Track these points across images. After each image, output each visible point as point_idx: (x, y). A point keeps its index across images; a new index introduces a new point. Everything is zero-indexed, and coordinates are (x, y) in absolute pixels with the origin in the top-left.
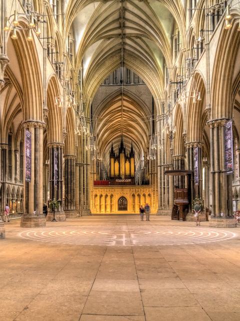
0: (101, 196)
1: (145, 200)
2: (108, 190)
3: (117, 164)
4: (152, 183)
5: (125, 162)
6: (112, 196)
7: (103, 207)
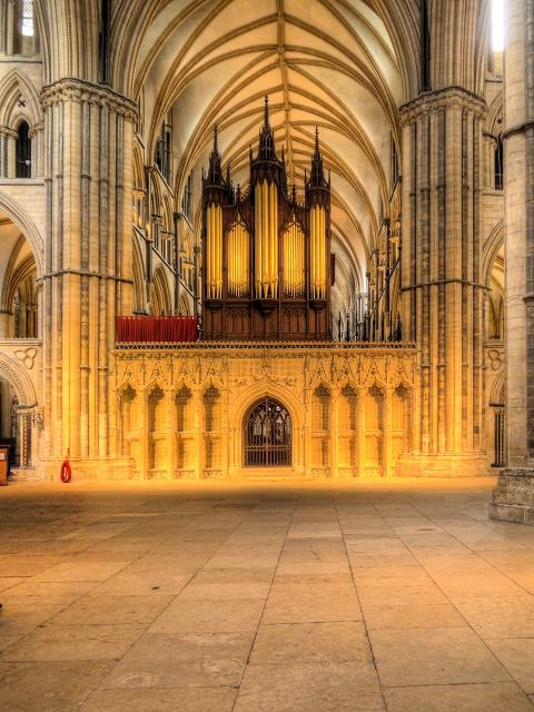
0: (155, 395)
1: (381, 415)
2: (191, 363)
3: (239, 236)
4: (413, 335)
5: (282, 229)
6: (211, 395)
7: (166, 449)
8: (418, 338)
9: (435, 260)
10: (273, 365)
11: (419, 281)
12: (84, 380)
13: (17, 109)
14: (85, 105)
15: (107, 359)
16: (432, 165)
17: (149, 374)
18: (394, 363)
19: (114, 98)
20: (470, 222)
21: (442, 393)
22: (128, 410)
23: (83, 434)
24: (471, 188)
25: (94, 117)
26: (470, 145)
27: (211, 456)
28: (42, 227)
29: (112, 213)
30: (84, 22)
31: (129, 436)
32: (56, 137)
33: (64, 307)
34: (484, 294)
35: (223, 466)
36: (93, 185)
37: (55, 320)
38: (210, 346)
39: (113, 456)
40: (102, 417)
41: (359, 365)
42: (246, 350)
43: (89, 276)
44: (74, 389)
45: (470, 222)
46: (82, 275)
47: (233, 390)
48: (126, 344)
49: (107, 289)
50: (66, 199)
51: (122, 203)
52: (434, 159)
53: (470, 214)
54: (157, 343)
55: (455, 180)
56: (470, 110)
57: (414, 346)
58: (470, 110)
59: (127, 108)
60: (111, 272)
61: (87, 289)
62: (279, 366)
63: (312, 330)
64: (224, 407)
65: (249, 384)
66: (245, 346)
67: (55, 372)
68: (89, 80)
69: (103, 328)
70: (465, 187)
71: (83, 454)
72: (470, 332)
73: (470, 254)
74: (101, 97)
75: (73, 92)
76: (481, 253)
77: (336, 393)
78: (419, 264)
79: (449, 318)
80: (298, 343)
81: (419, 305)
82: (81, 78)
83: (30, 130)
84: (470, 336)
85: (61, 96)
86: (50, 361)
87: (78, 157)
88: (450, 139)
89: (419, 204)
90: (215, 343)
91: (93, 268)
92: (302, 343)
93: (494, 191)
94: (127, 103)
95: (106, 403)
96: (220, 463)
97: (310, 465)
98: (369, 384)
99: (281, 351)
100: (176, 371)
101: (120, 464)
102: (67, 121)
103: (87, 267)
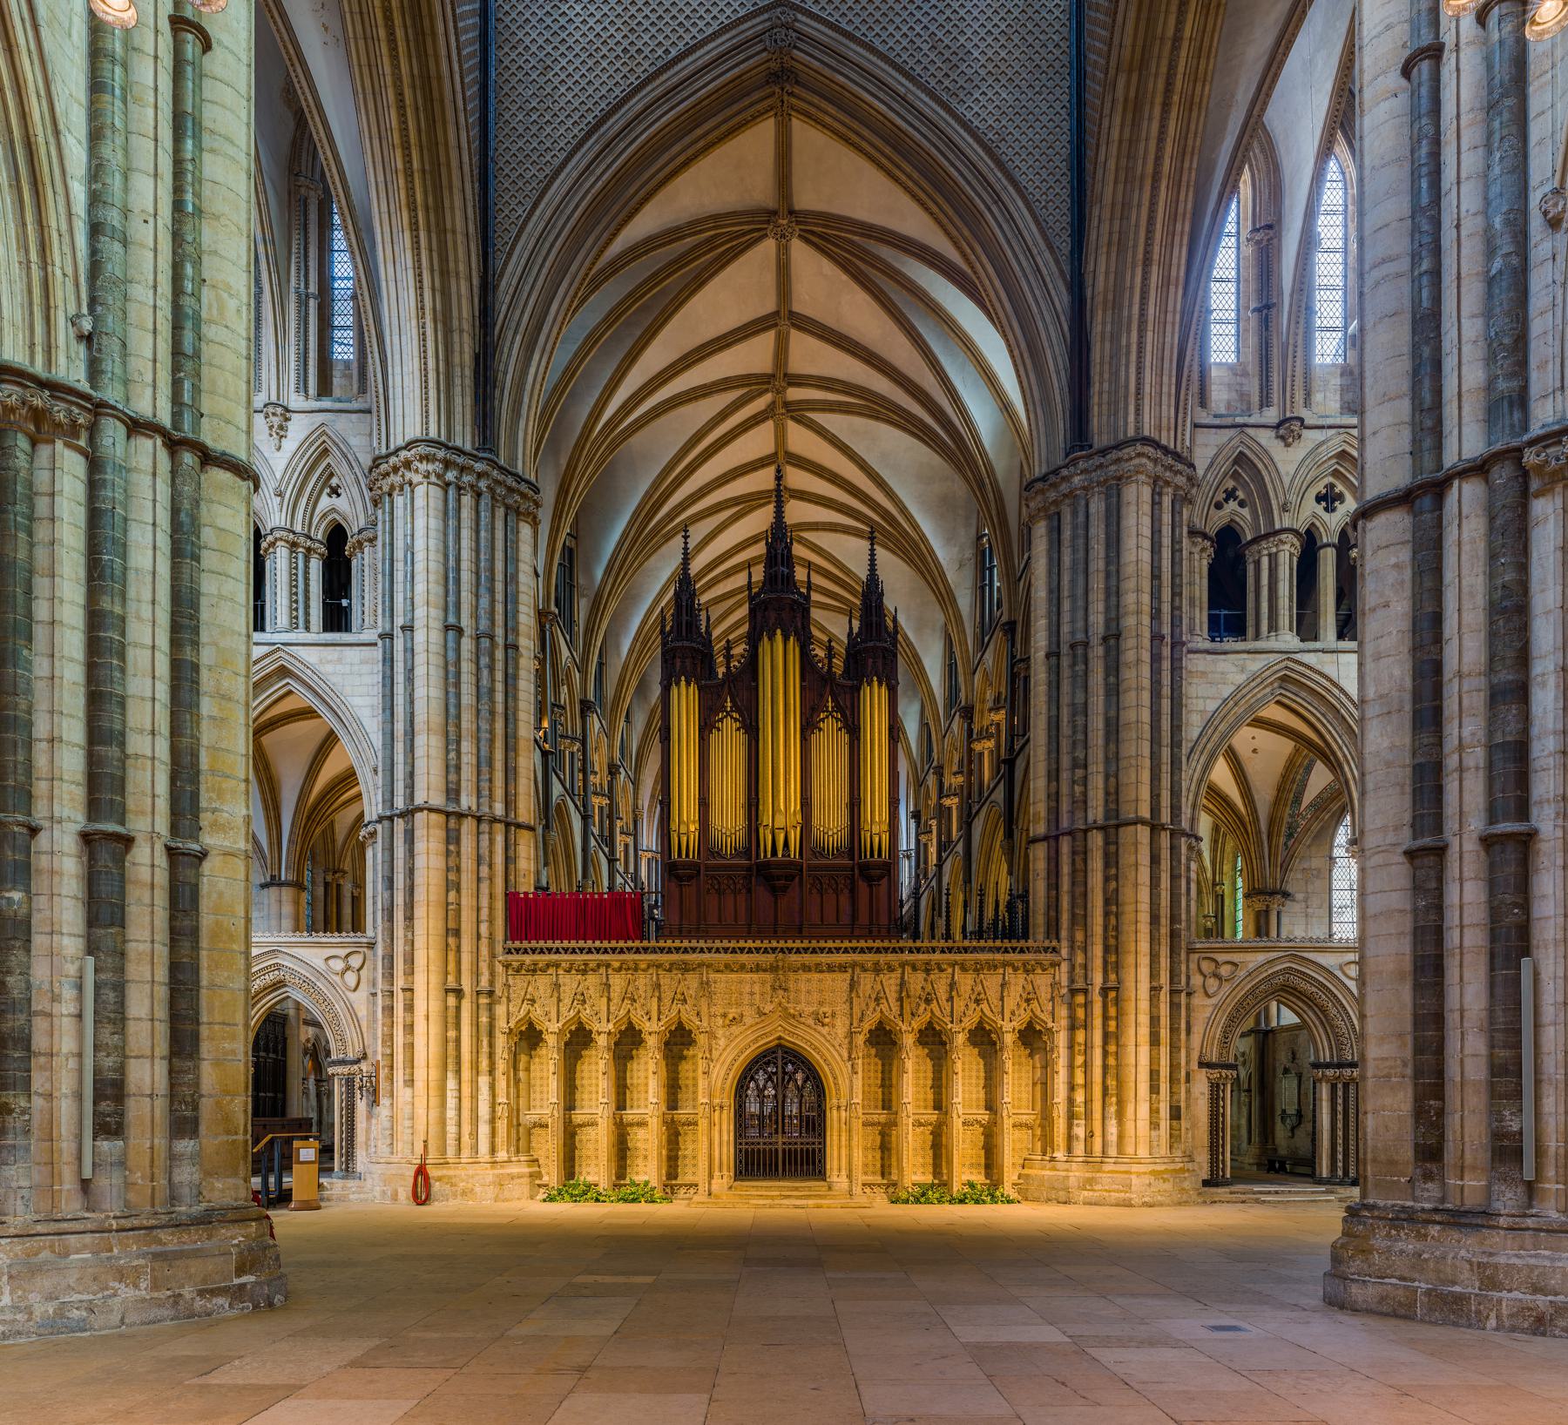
0: (578, 1040)
1: (991, 1083)
2: (643, 981)
4: (1053, 929)
6: (678, 1042)
8: (1064, 934)
9: (1097, 783)
10: (791, 985)
11: (1065, 823)
12: (451, 1013)
13: (325, 502)
14: (452, 492)
15: (492, 974)
16: (1092, 597)
17: (567, 1001)
18: (1018, 981)
19: (501, 477)
20: (1166, 704)
21: (1113, 1041)
22: (528, 1070)
23: (451, 1113)
24: (1168, 639)
25: (466, 514)
26: (1166, 554)
27: (676, 1158)
28: (373, 726)
29: (499, 697)
30: (448, 332)
31: (528, 1118)
32: (399, 554)
33: (417, 873)
34: (1190, 848)
35: (701, 1177)
36: (467, 644)
37: (399, 899)
38: (678, 950)
39: (502, 1155)
40: (484, 1081)
41: (952, 985)
42: (744, 958)
43: (461, 816)
44: (435, 1029)
45: (1166, 704)
46: (448, 814)
47: (720, 1033)
48: (525, 944)
49: (492, 842)
50: (420, 671)
51: (516, 677)
52: (1098, 583)
53: (1166, 691)
54: (581, 944)
55: (1139, 623)
56: (1167, 483)
57: (1054, 950)
58: (1167, 483)
59: (523, 496)
60: (499, 809)
61: (458, 842)
62: (803, 986)
63: (864, 918)
64: (701, 1065)
65: (748, 1020)
66: (742, 950)
67: (400, 999)
68: (459, 443)
69: (485, 913)
70: (1156, 637)
71: (451, 1151)
72: (1164, 921)
73: (1166, 768)
74: (480, 475)
75: (430, 467)
76: (1184, 767)
77: (909, 1040)
78: (1064, 789)
79: (1127, 894)
80: (838, 944)
81: (1066, 869)
82: (443, 439)
83: (351, 542)
84: (1164, 930)
85: (408, 475)
86: (389, 976)
87: (441, 590)
88: (1129, 543)
89: (1066, 672)
90: (686, 944)
91: (467, 801)
92: (846, 944)
93: (1208, 645)
94: (523, 487)
95: (491, 1055)
96: (694, 1170)
97: (860, 1178)
98: (970, 1022)
99: (808, 958)
100: (616, 993)
101: (514, 1169)
102: (420, 523)
103: (458, 801)
